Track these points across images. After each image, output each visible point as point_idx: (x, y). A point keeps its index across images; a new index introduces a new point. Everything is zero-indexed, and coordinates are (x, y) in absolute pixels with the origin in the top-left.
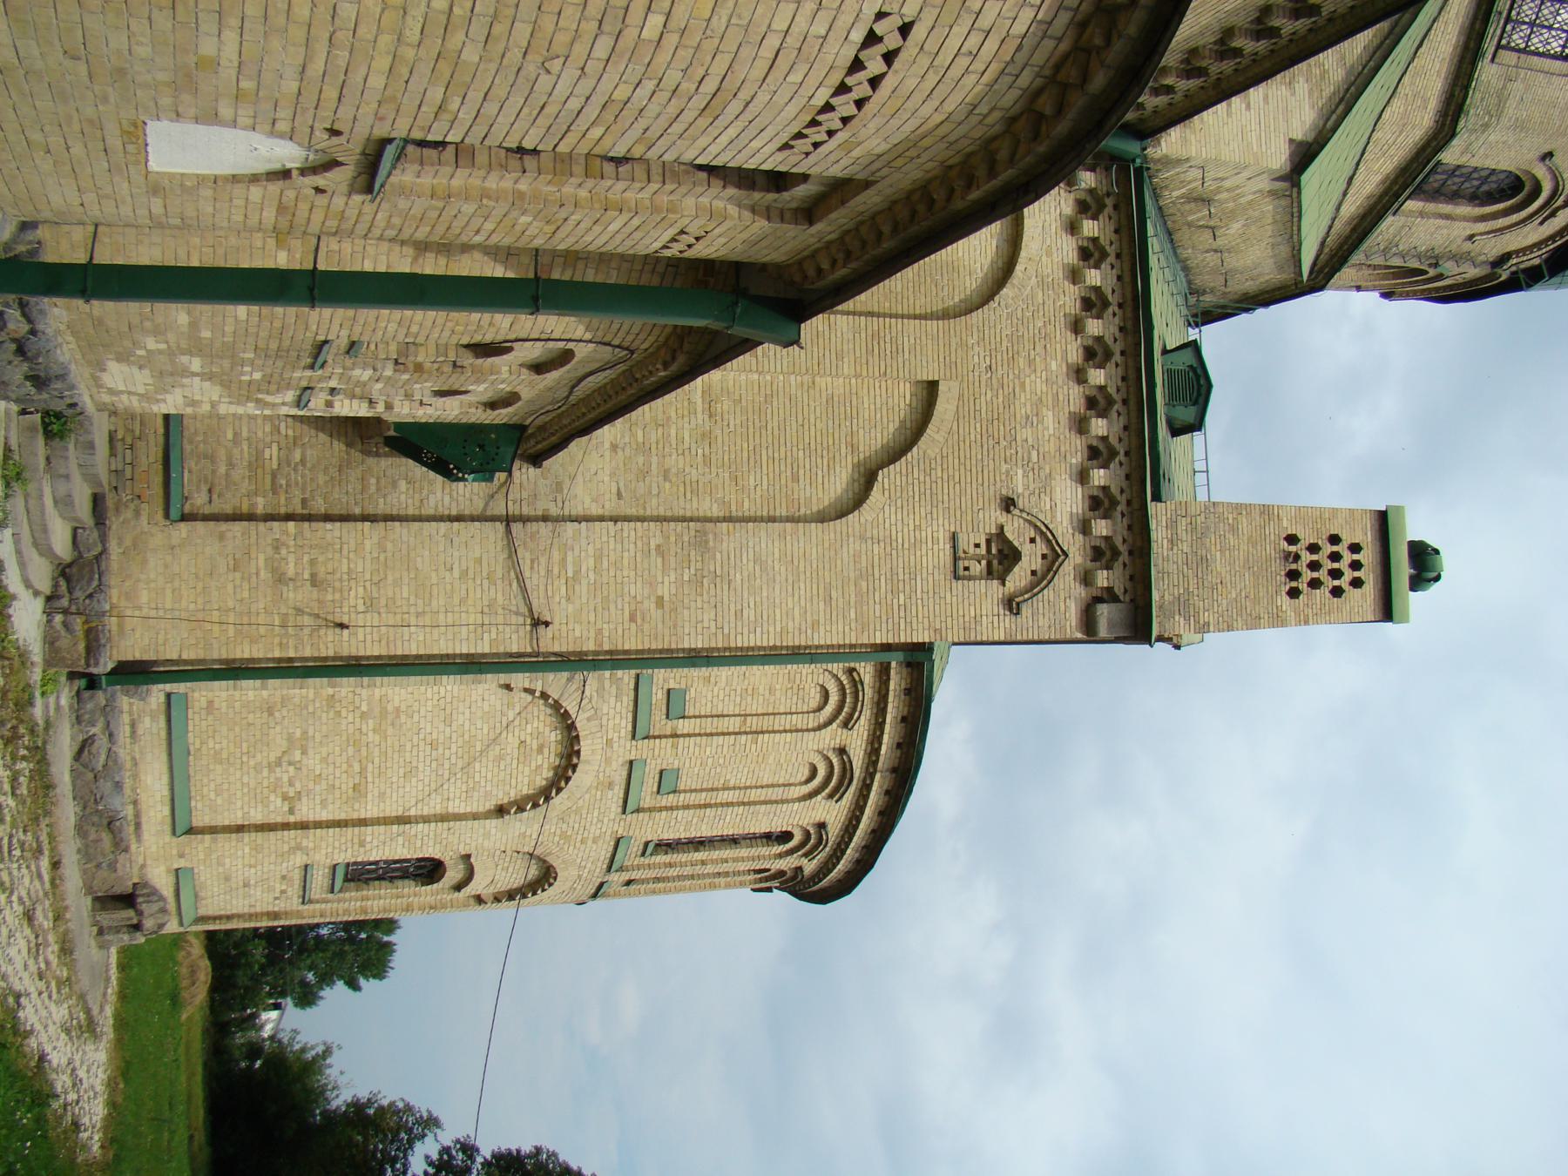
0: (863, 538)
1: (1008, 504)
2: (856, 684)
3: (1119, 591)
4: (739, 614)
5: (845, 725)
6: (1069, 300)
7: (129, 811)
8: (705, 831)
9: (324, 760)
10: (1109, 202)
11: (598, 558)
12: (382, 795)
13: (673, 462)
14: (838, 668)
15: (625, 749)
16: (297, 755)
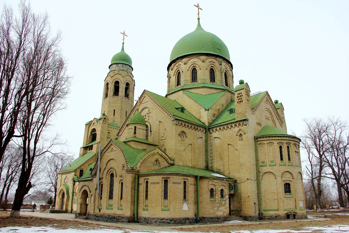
0: (240, 150)
1: (237, 135)
2: (260, 144)
3: (242, 123)
4: (247, 161)
5: (265, 144)
6: (221, 131)
7: (275, 215)
8: (287, 154)
9: (270, 196)
10: (212, 129)
11: (243, 174)
12: (274, 191)
13: (236, 168)
14: (258, 146)
15: (268, 167)
16: (270, 199)
